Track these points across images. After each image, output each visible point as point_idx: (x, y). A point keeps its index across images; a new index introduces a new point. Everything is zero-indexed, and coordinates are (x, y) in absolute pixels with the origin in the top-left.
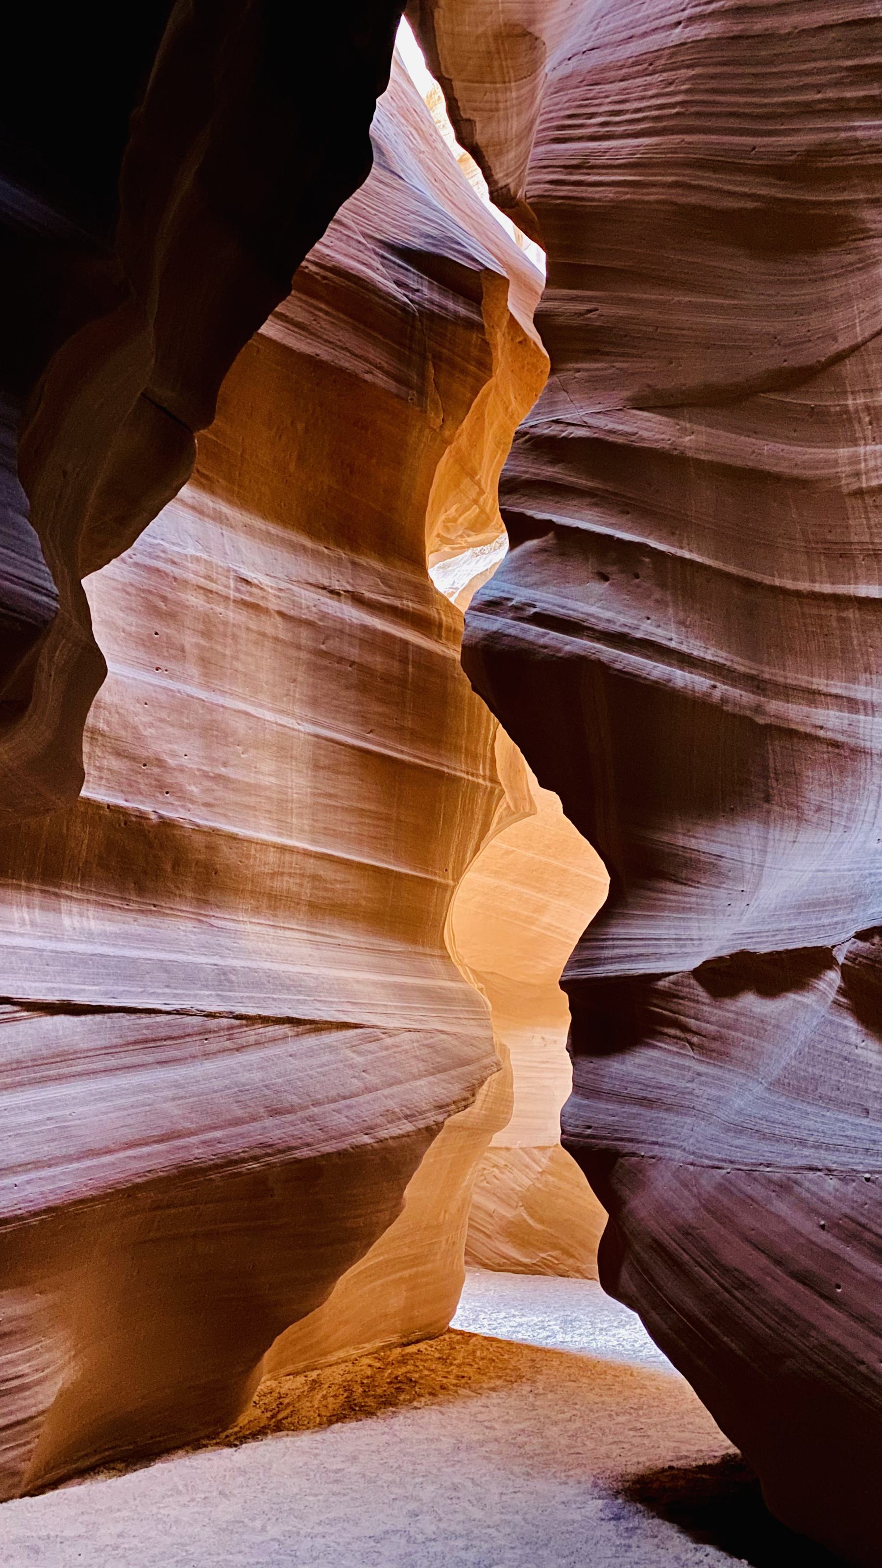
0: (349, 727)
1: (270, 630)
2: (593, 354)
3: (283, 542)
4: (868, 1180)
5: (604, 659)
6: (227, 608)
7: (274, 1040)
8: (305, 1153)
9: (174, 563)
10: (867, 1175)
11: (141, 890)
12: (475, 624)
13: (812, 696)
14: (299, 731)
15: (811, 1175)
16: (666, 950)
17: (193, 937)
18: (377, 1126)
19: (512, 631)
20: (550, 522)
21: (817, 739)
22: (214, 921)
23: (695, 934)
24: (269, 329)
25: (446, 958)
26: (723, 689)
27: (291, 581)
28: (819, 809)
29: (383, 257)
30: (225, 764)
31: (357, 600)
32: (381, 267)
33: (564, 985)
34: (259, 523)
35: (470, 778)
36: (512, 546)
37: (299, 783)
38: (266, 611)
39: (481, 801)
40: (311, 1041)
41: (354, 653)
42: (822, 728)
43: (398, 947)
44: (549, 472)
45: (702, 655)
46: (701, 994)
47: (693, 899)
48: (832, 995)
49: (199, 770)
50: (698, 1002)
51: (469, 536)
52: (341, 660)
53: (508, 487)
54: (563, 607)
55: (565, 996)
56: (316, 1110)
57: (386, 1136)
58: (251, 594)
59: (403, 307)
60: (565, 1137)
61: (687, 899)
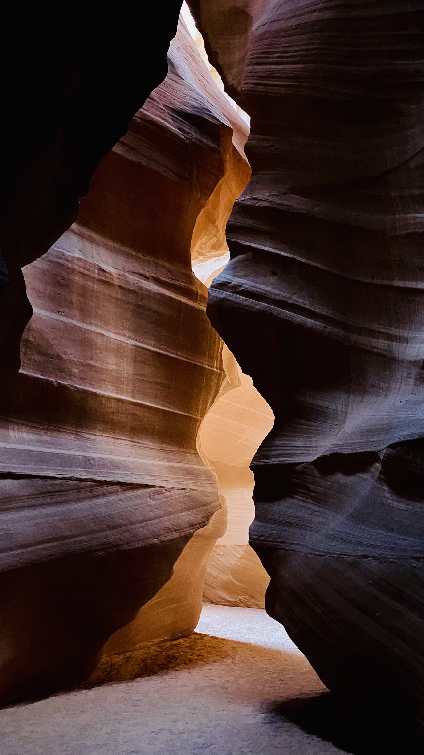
0: (152, 342)
1: (114, 295)
4: (392, 562)
5: (274, 313)
6: (93, 283)
7: (112, 493)
8: (126, 547)
9: (68, 260)
10: (392, 560)
12: (214, 294)
13: (372, 333)
14: (127, 344)
15: (366, 560)
16: (300, 452)
17: (74, 442)
18: (161, 535)
19: (231, 298)
20: (250, 246)
21: (374, 353)
22: (84, 435)
23: (314, 444)
24: (117, 149)
25: (196, 454)
26: (329, 328)
27: (125, 271)
28: (373, 386)
29: (173, 116)
30: (91, 359)
31: (158, 281)
32: (172, 121)
33: (252, 468)
34: (110, 243)
35: (210, 368)
36: (232, 258)
37: (127, 369)
38: (113, 285)
39: (214, 379)
40: (130, 494)
41: (155, 306)
42: (375, 348)
43: (173, 449)
44: (249, 222)
45: (320, 312)
46: (317, 473)
47: (314, 428)
48: (377, 474)
49: (78, 361)
50: (315, 477)
51: (212, 252)
52: (149, 310)
53: (230, 229)
54: (255, 287)
55: (252, 473)
56: (132, 527)
57: (165, 540)
58: (106, 277)
60: (250, 540)
61: (311, 428)
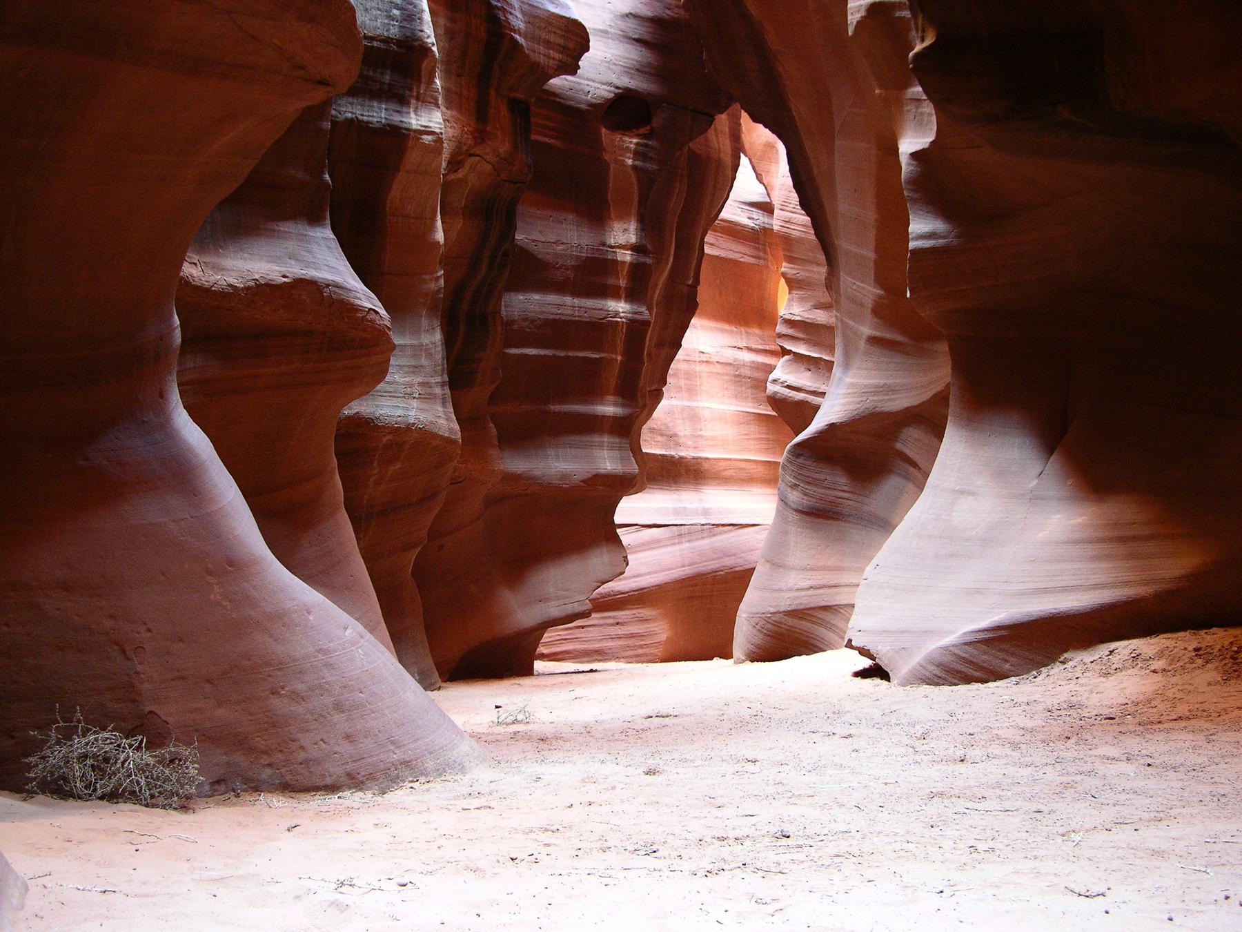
1: (715, 370)
2: (800, 288)
3: (717, 329)
11: (675, 482)
31: (750, 349)
41: (748, 373)
44: (790, 331)
59: (752, 228)
